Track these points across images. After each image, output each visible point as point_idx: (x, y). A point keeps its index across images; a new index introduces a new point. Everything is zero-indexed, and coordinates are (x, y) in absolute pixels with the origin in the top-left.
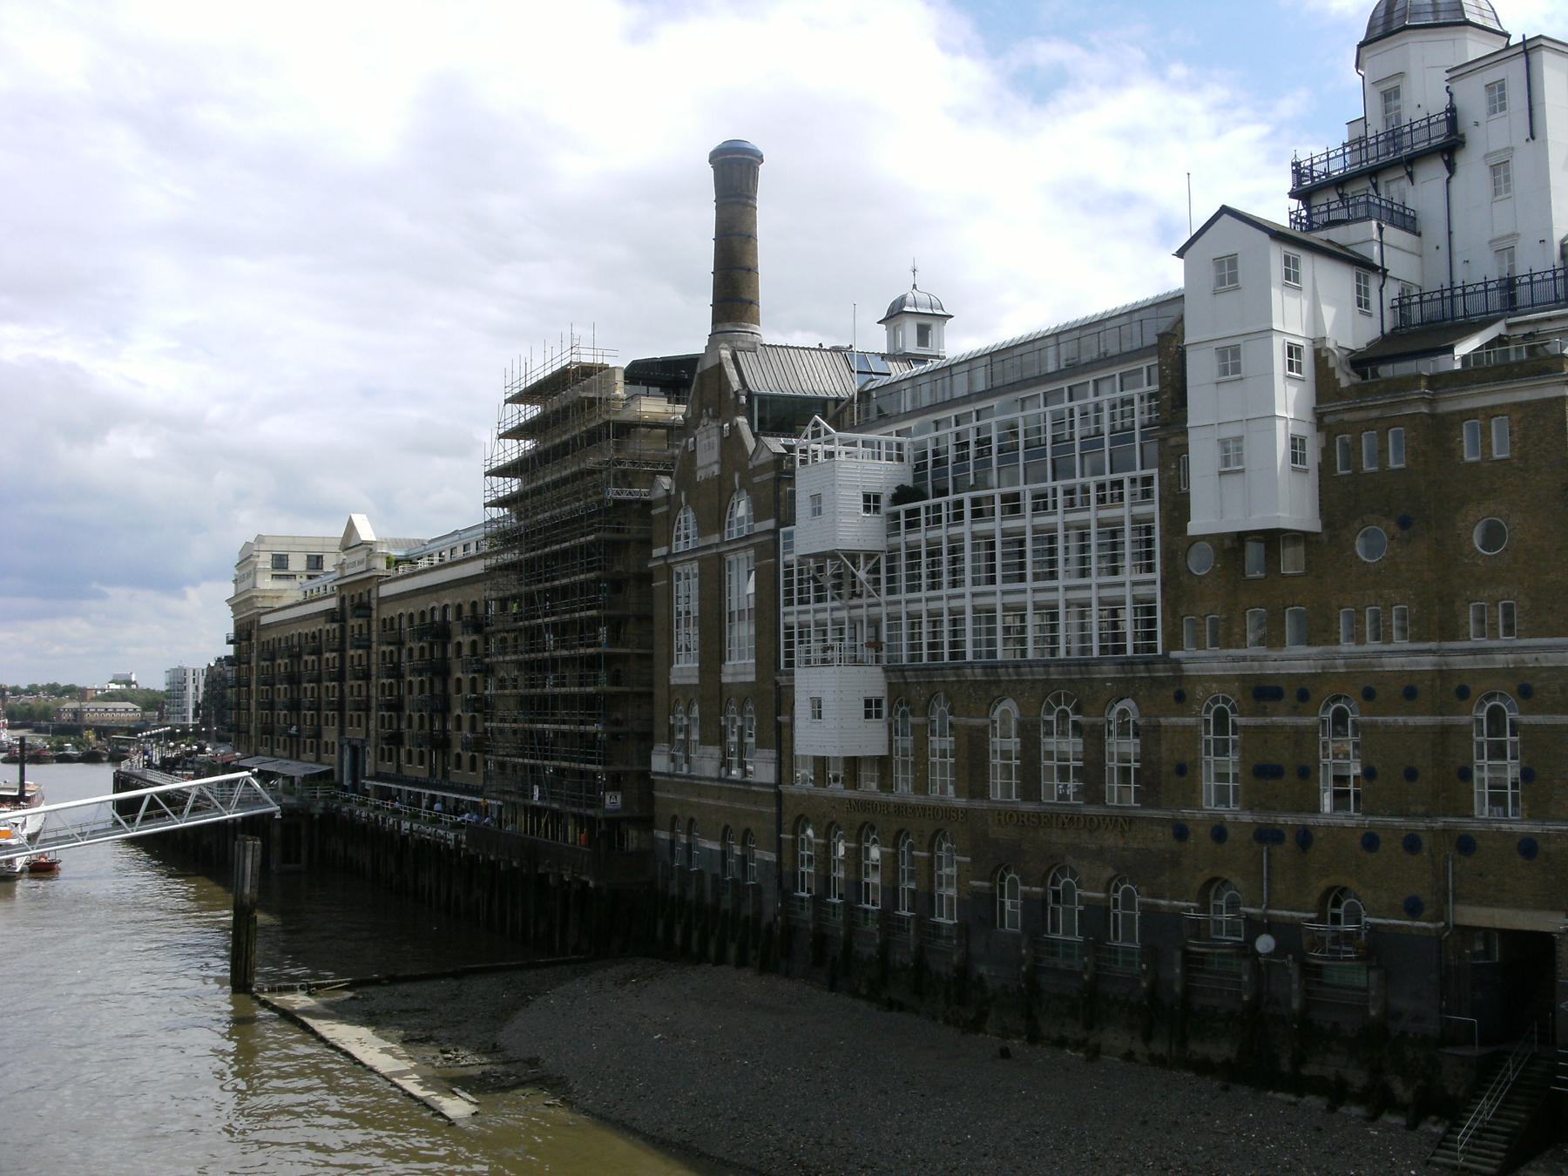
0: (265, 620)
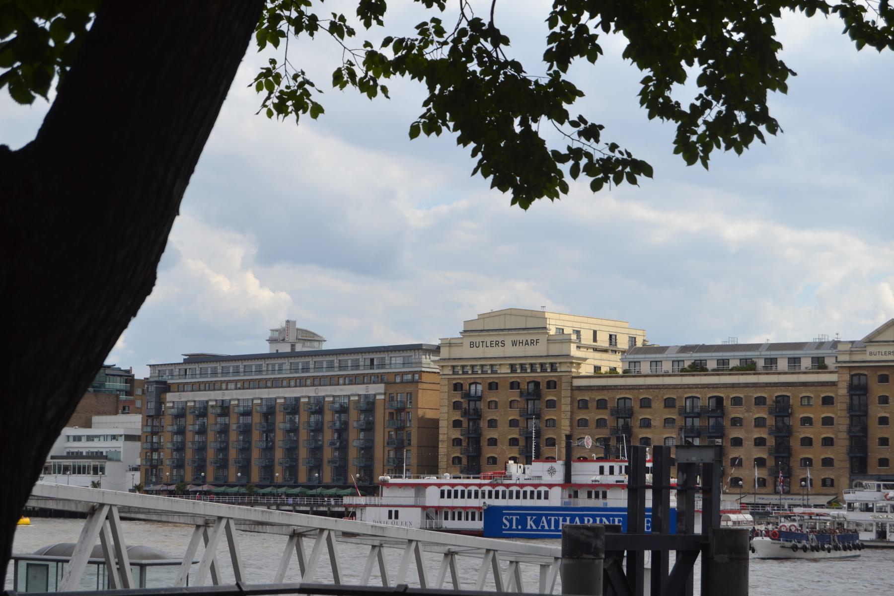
0: (577, 383)
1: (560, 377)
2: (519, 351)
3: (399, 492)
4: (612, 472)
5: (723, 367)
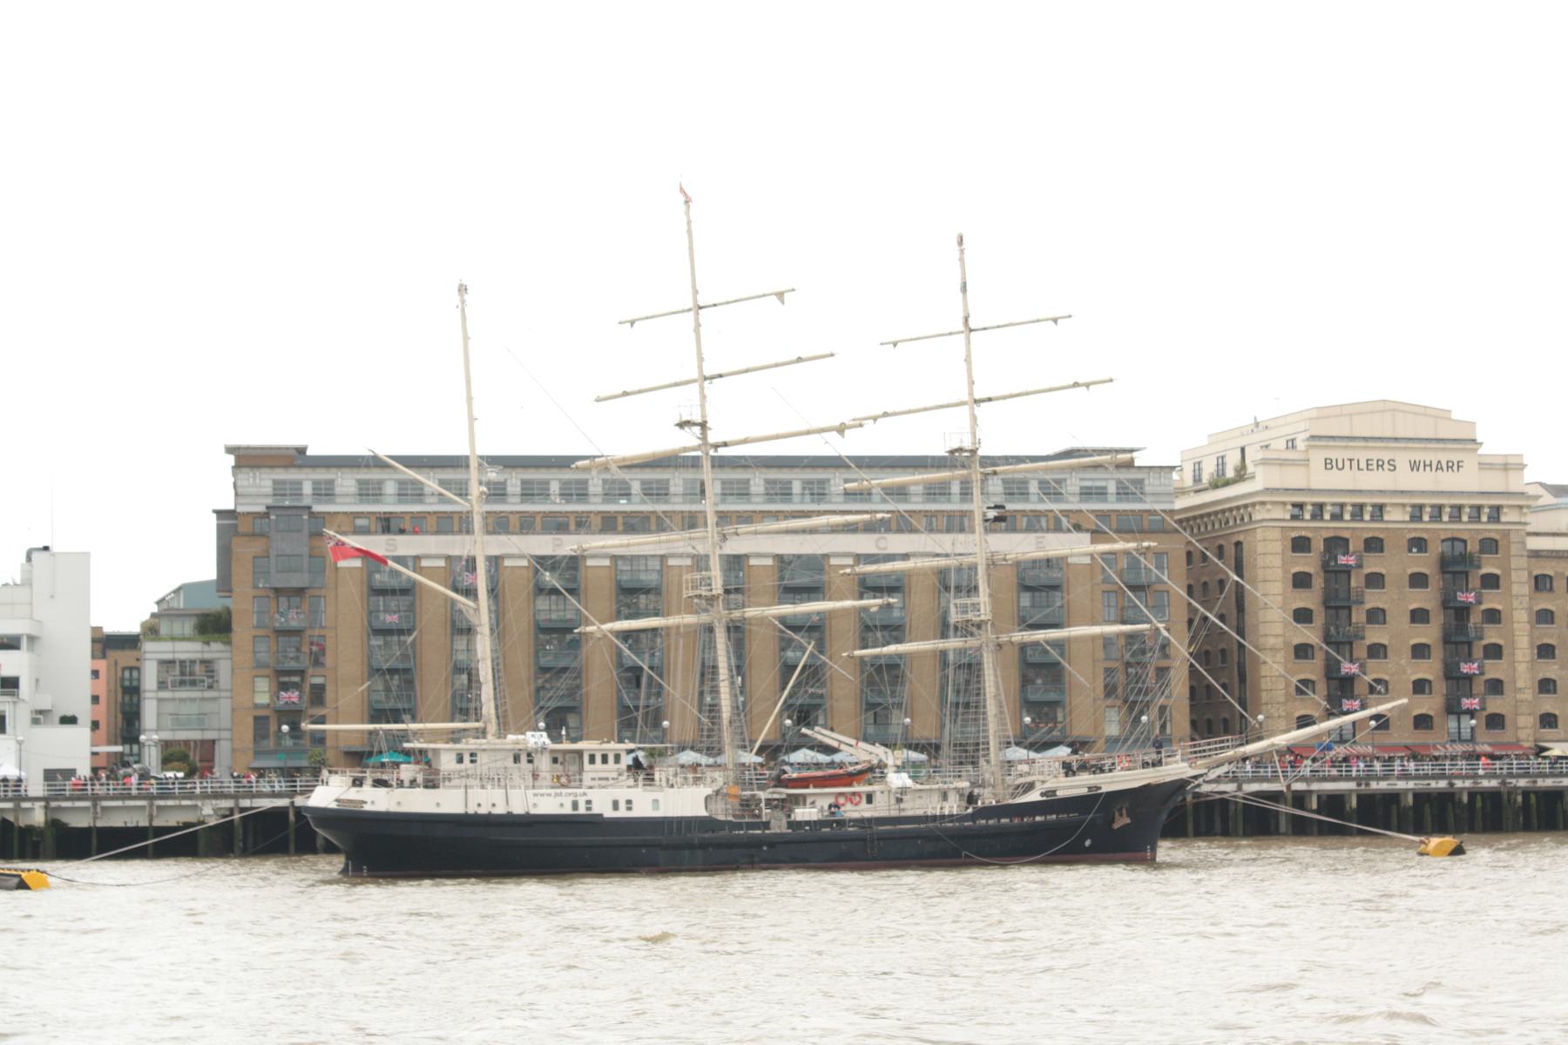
1: (1506, 533)
2: (1424, 481)
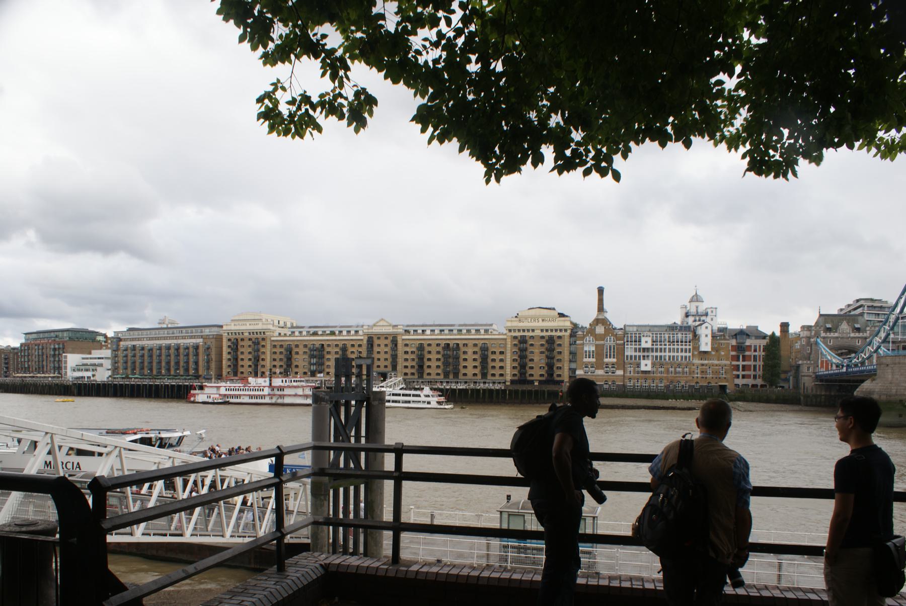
0: (273, 339)
2: (252, 327)
3: (211, 389)
4: (286, 381)
5: (324, 334)
